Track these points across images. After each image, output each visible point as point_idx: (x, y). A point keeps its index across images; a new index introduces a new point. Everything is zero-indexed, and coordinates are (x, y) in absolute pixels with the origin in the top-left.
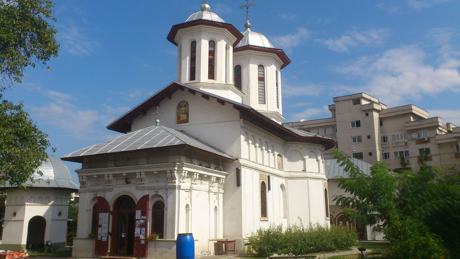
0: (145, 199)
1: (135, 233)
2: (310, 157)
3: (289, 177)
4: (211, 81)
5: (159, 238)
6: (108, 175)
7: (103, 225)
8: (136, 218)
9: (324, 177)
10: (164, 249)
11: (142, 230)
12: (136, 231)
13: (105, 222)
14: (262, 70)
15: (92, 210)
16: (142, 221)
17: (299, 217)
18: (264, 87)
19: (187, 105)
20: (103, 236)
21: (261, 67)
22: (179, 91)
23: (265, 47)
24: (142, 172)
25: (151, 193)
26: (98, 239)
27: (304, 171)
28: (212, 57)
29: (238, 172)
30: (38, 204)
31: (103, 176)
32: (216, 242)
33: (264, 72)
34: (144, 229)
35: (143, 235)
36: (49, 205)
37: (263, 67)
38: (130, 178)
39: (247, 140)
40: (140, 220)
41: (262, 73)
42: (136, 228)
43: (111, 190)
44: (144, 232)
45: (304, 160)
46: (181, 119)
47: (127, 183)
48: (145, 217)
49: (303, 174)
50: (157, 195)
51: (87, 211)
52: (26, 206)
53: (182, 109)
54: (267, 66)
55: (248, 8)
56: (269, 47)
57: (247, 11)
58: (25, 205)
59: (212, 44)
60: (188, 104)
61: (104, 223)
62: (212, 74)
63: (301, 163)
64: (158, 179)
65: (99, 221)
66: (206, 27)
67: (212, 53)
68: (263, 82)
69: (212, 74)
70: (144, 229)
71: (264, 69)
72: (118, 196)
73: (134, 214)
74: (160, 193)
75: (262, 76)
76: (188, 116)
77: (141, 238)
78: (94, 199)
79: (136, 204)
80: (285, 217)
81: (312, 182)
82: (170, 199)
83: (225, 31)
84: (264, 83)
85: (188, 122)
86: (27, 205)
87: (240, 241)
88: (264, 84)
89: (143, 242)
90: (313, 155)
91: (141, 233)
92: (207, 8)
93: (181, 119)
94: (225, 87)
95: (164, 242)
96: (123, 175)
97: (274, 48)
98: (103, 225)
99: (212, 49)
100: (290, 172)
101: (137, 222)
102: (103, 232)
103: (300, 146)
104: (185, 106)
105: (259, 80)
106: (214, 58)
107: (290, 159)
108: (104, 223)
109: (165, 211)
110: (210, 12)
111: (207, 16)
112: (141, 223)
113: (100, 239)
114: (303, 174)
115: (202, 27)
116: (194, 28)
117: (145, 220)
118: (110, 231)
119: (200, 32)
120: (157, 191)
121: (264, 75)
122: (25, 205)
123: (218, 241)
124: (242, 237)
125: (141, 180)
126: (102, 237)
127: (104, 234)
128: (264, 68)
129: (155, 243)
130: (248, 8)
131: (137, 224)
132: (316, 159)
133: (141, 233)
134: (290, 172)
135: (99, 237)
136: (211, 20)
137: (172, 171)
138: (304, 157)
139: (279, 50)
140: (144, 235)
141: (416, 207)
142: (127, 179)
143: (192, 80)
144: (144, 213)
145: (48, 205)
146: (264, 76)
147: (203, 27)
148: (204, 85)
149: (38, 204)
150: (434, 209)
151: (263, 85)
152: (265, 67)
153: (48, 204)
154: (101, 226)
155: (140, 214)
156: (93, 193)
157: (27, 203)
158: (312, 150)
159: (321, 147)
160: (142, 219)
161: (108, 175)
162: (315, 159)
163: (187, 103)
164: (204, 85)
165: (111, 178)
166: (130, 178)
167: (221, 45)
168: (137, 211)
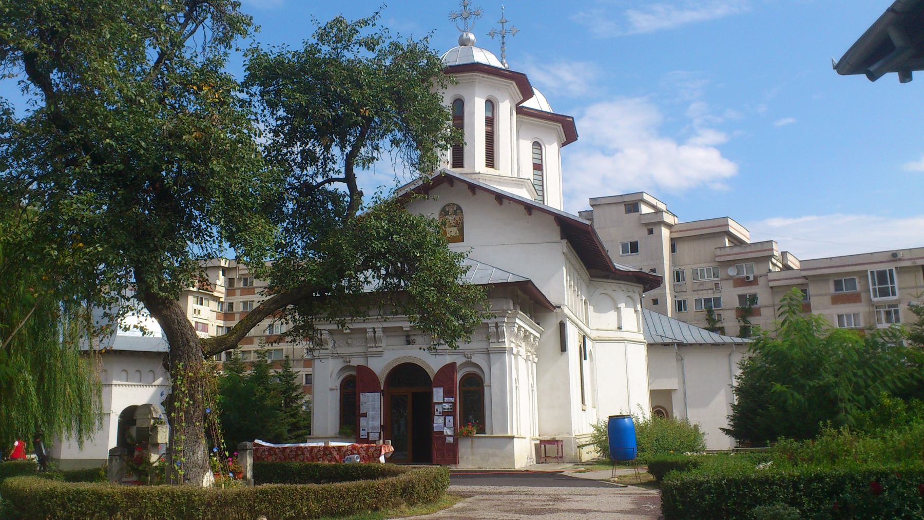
0: (450, 368)
1: (435, 425)
2: (627, 306)
3: (597, 338)
4: (491, 171)
5: (477, 433)
6: (374, 329)
7: (370, 413)
8: (435, 401)
9: (641, 337)
10: (490, 451)
11: (447, 421)
12: (435, 421)
13: (374, 408)
14: (539, 152)
15: (339, 388)
16: (447, 406)
17: (638, 405)
18: (542, 181)
19: (458, 210)
20: (370, 431)
21: (537, 145)
22: (445, 185)
23: (543, 110)
24: (378, 328)
25: (460, 360)
26: (361, 437)
27: (620, 328)
28: (490, 129)
29: (562, 327)
30: (130, 383)
31: (364, 331)
32: (538, 442)
33: (541, 154)
34: (451, 418)
35: (449, 428)
36: (155, 385)
37: (540, 146)
38: (414, 335)
39: (568, 273)
40: (441, 403)
41: (539, 157)
42: (436, 417)
43: (379, 354)
44: (451, 424)
45: (618, 310)
46: (448, 235)
47: (408, 343)
48: (452, 400)
49: (618, 334)
50: (469, 363)
51: (331, 389)
52: (114, 389)
53: (451, 218)
54: (546, 145)
55: (503, 37)
56: (549, 111)
57: (501, 42)
58: (112, 385)
59: (491, 105)
60: (462, 210)
61: (371, 410)
62: (491, 161)
63: (613, 314)
64: (350, 341)
65: (361, 407)
66: (483, 77)
67: (490, 122)
68: (540, 173)
69: (491, 161)
70: (451, 418)
71: (541, 149)
72: (394, 365)
73: (430, 395)
74: (475, 359)
75: (538, 162)
76: (461, 230)
77: (445, 433)
78: (343, 369)
79: (432, 380)
80: (594, 407)
81: (631, 347)
82: (495, 369)
83: (512, 86)
84: (542, 174)
85: (463, 241)
86: (115, 385)
87: (569, 440)
88: (542, 176)
89: (450, 440)
90: (631, 301)
91: (445, 425)
92: (472, 40)
93: (448, 235)
94: (519, 183)
95: (488, 440)
96: (404, 329)
97: (552, 112)
98: (370, 413)
99: (490, 115)
100: (597, 330)
101: (436, 407)
102: (370, 426)
103: (614, 286)
104: (455, 213)
105: (534, 169)
106: (493, 131)
107: (597, 310)
108: (371, 410)
109: (486, 390)
110: (483, 50)
111: (482, 56)
112: (445, 409)
113: (366, 437)
114: (618, 334)
115: (477, 75)
116: (463, 76)
117: (451, 404)
118: (382, 424)
119: (472, 83)
120: (469, 356)
121: (541, 160)
122: (112, 385)
123: (540, 441)
124: (572, 434)
125: (375, 339)
126: (368, 433)
127: (373, 428)
128: (541, 148)
129: (472, 441)
130: (503, 37)
131: (437, 411)
132: (633, 309)
133: (445, 425)
134: (597, 330)
135: (362, 433)
136: (488, 64)
137: (499, 325)
138: (619, 306)
139: (569, 117)
140: (452, 429)
141: (870, 382)
142: (408, 336)
143: (457, 167)
144: (448, 393)
145: (152, 386)
146: (542, 162)
147: (478, 76)
148: (485, 178)
149: (130, 383)
150: (896, 386)
151: (540, 178)
152: (543, 147)
153: (154, 384)
154: (365, 415)
155: (442, 394)
156: (341, 360)
157: (114, 382)
158: (630, 294)
159: (639, 288)
160: (446, 403)
161: (374, 329)
162: (633, 310)
163: (459, 208)
164: (486, 178)
165: (379, 334)
166: (414, 335)
167: (505, 110)
168: (435, 390)
